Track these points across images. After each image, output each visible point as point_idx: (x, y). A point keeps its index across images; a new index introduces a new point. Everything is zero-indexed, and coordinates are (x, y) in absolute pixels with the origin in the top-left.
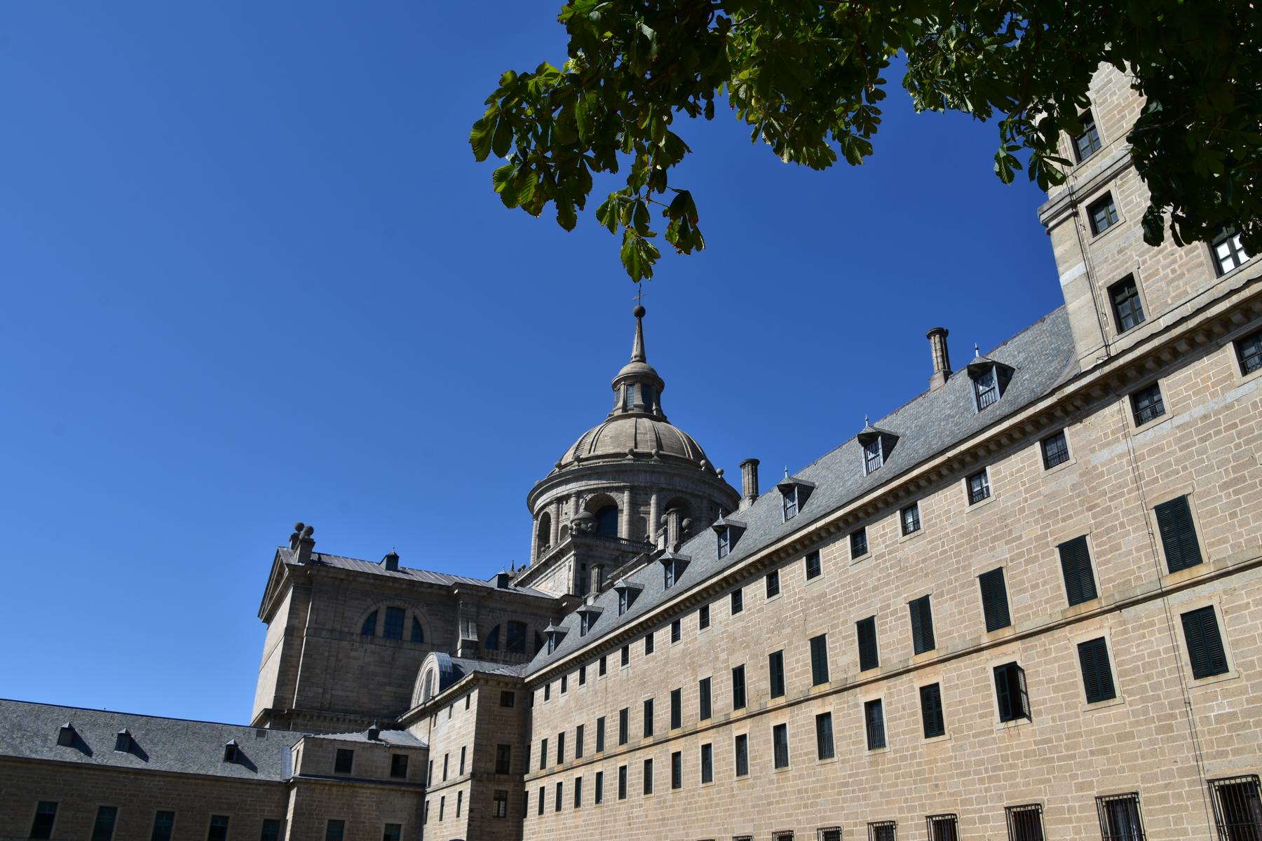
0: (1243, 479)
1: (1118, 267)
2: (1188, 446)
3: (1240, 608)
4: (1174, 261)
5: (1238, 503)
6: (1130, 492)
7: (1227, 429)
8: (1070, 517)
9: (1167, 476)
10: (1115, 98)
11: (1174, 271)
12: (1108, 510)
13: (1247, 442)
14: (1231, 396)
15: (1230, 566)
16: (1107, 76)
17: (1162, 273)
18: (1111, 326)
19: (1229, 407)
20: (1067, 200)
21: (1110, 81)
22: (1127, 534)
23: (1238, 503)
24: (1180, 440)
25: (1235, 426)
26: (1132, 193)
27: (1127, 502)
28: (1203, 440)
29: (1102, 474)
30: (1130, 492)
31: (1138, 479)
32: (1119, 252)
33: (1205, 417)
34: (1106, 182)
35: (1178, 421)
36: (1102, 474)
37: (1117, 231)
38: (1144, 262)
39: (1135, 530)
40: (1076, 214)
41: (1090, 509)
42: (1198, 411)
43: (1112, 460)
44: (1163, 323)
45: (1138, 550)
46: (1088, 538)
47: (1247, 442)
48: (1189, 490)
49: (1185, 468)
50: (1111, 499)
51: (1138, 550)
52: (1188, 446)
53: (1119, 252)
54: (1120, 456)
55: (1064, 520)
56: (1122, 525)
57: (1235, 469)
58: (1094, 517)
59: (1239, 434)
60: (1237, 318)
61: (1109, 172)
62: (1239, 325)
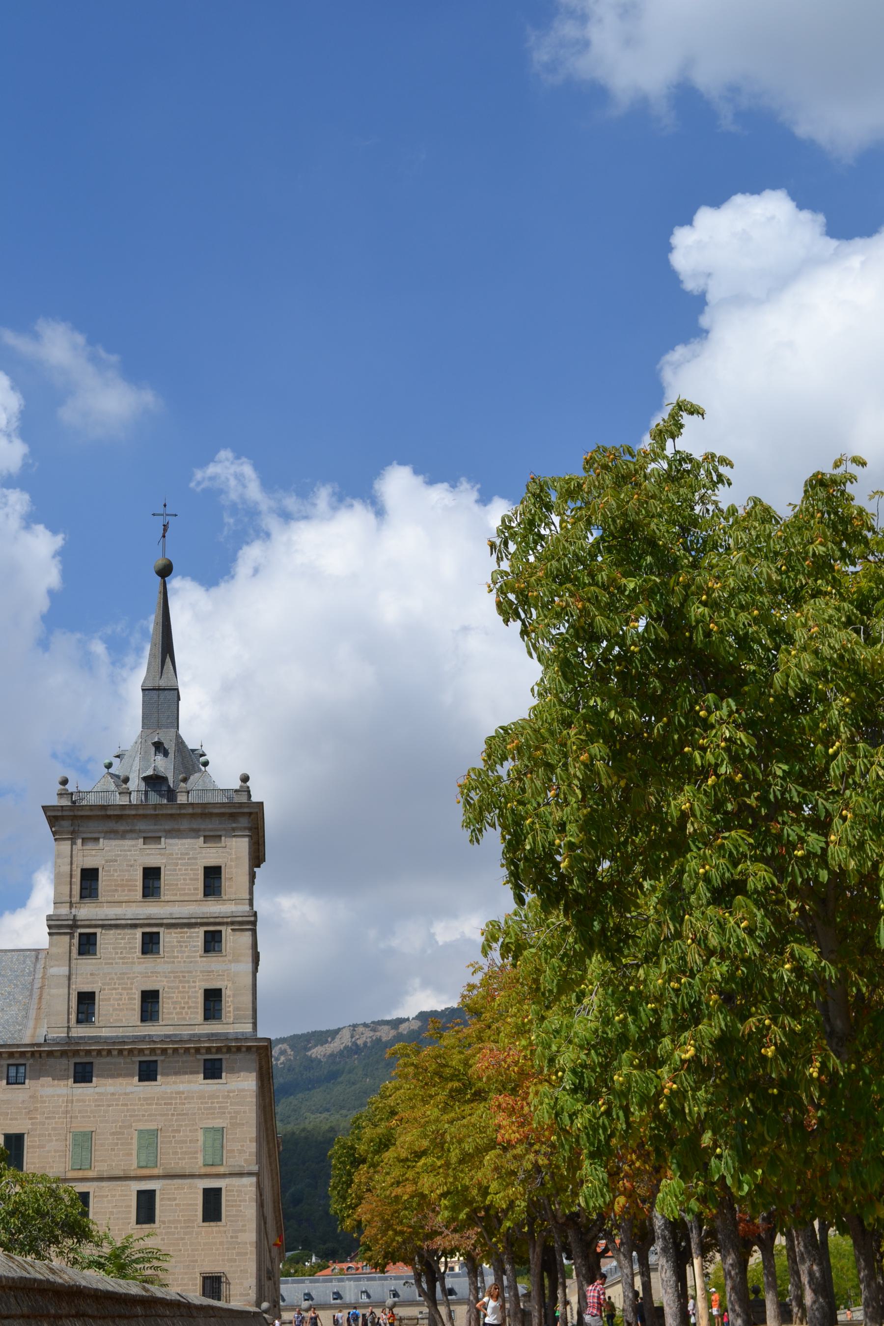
0: (123, 1134)
1: (88, 983)
2: (99, 1106)
3: (102, 1196)
4: (121, 999)
5: (117, 1144)
6: (59, 1118)
7: (122, 1105)
8: (16, 1119)
9: (83, 1117)
10: (116, 874)
11: (119, 1005)
12: (43, 1124)
13: (131, 1116)
14: (129, 1089)
15: (105, 1175)
16: (115, 855)
17: (112, 1002)
18: (73, 1017)
19: (126, 1094)
20: (70, 922)
21: (116, 861)
22: (51, 1141)
23: (117, 1144)
24: (96, 1100)
25: (126, 1105)
26: (110, 944)
27: (56, 1123)
28: (109, 1106)
29: (45, 1102)
30: (59, 1118)
31: (67, 1112)
32: (91, 974)
33: (113, 1094)
34: (96, 926)
35: (97, 1090)
36: (45, 1102)
37: (94, 961)
38: (104, 989)
39: (56, 1140)
40: (71, 935)
41: (31, 1119)
42: (111, 1089)
43: (53, 1096)
44: (105, 1033)
45: (55, 1151)
46: (26, 1136)
47: (131, 1116)
48: (94, 1129)
49: (94, 1117)
50: (46, 1118)
51: (55, 1151)
52: (99, 1106)
53: (91, 974)
54: (59, 1096)
55: (11, 1119)
56: (49, 1135)
57: (120, 1127)
58: (32, 1124)
59: (128, 1111)
60: (147, 1052)
61: (100, 922)
62: (144, 1055)
